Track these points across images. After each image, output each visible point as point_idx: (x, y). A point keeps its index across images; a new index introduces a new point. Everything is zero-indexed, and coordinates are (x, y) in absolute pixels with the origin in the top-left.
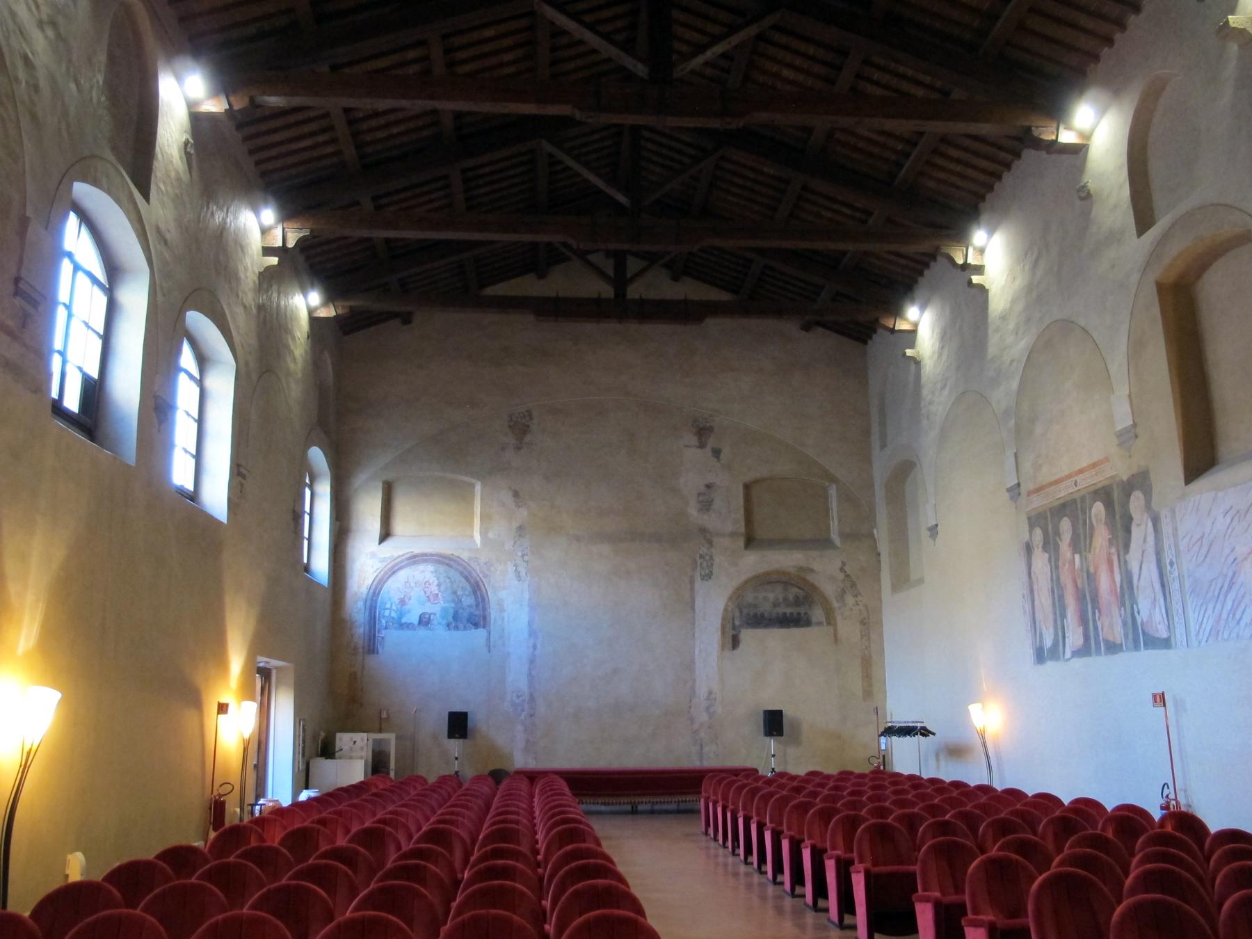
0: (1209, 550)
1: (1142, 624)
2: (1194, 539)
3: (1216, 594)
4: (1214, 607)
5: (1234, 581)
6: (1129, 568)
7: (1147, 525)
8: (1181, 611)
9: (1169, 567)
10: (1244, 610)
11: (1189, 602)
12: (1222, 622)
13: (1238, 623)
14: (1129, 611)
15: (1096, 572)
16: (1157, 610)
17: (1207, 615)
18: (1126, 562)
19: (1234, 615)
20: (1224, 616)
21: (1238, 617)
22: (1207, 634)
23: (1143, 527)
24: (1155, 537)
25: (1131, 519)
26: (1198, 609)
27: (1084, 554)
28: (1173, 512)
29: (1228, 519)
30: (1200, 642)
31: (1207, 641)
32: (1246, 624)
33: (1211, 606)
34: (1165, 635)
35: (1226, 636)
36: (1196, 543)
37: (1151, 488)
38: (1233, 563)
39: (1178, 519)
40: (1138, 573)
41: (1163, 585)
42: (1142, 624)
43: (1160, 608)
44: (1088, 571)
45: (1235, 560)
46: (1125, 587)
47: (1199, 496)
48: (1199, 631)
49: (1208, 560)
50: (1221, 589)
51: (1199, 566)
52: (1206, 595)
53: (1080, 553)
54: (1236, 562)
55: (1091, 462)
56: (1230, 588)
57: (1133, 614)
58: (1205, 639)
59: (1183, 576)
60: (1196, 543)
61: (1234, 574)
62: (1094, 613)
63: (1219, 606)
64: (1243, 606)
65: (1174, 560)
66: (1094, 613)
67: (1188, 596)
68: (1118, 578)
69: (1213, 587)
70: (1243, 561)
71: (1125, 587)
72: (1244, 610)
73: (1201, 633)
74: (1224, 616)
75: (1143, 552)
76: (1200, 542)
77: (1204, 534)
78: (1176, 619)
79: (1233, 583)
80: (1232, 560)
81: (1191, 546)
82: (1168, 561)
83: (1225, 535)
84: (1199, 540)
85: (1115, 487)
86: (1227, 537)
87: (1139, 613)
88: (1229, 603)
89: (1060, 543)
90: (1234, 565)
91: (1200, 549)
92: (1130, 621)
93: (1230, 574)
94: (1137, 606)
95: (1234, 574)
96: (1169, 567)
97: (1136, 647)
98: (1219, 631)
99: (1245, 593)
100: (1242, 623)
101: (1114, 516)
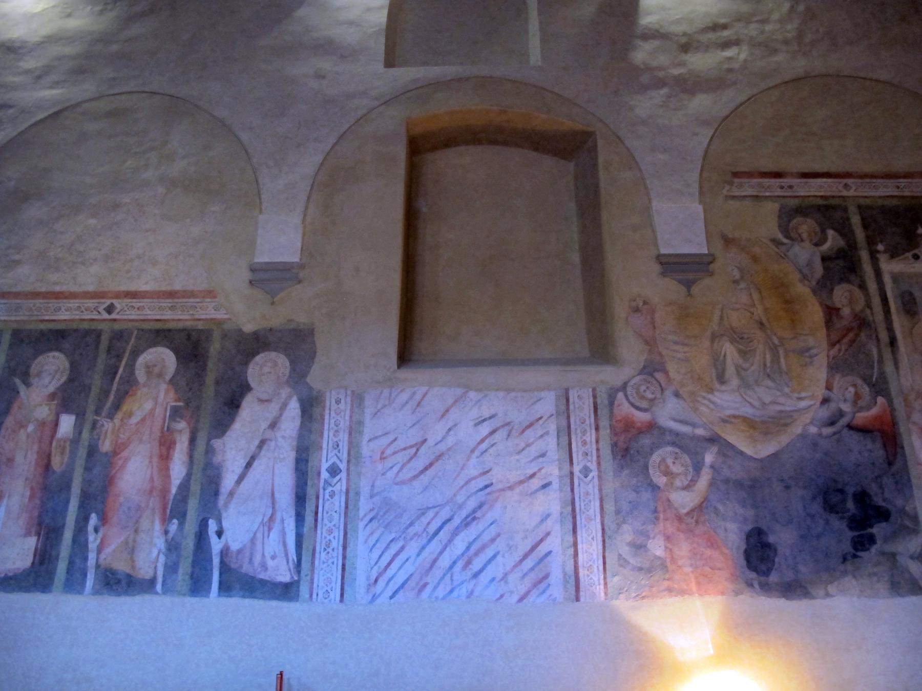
0: (431, 465)
1: (225, 552)
2: (401, 444)
3: (432, 528)
4: (423, 548)
5: (478, 514)
6: (217, 459)
7: (284, 406)
8: (337, 544)
9: (325, 475)
10: (494, 556)
11: (362, 535)
12: (437, 573)
13: (476, 575)
14: (191, 526)
15: (115, 453)
16: (274, 535)
17: (402, 557)
18: (210, 451)
19: (468, 563)
20: (445, 561)
21: (477, 565)
22: (393, 586)
23: (274, 408)
24: (303, 426)
25: (246, 388)
26: (381, 546)
27: (90, 417)
28: (358, 399)
29: (485, 429)
30: (374, 598)
31: (391, 598)
32: (493, 579)
33: (412, 549)
34: (284, 576)
35: (441, 592)
36: (405, 449)
37: (313, 355)
38: (481, 490)
39: (368, 412)
40: (239, 471)
41: (300, 499)
42: (225, 552)
43: (283, 533)
44: (92, 451)
45: (486, 487)
46: (195, 488)
47: (424, 389)
48: (376, 581)
49: (425, 478)
50: (444, 523)
51: (403, 483)
52: (407, 528)
53: (81, 416)
54: (489, 490)
55: (169, 288)
56: (468, 521)
57: (201, 537)
58: (389, 593)
59: (358, 494)
60: (405, 449)
61: (480, 506)
62: (83, 519)
63: (435, 546)
64: (489, 552)
65: (343, 466)
66: (83, 519)
67: (361, 525)
68: (178, 470)
69: (425, 520)
70: (503, 490)
71: (195, 488)
72: (494, 556)
73: (381, 583)
74: (445, 561)
75: (263, 443)
76: (414, 450)
77: (425, 440)
78: (321, 556)
79: (474, 519)
80: (481, 485)
81: (389, 452)
82: (325, 466)
83: (473, 451)
84: (411, 447)
85: (216, 335)
86: (477, 453)
87: (220, 534)
88: (460, 545)
89: (22, 389)
90: (481, 493)
91: (411, 459)
92: (189, 544)
93: (472, 504)
94: (219, 522)
95: (480, 506)
96: (325, 475)
97: (198, 586)
98: (426, 585)
99: (499, 535)
100: (484, 578)
101: (200, 374)
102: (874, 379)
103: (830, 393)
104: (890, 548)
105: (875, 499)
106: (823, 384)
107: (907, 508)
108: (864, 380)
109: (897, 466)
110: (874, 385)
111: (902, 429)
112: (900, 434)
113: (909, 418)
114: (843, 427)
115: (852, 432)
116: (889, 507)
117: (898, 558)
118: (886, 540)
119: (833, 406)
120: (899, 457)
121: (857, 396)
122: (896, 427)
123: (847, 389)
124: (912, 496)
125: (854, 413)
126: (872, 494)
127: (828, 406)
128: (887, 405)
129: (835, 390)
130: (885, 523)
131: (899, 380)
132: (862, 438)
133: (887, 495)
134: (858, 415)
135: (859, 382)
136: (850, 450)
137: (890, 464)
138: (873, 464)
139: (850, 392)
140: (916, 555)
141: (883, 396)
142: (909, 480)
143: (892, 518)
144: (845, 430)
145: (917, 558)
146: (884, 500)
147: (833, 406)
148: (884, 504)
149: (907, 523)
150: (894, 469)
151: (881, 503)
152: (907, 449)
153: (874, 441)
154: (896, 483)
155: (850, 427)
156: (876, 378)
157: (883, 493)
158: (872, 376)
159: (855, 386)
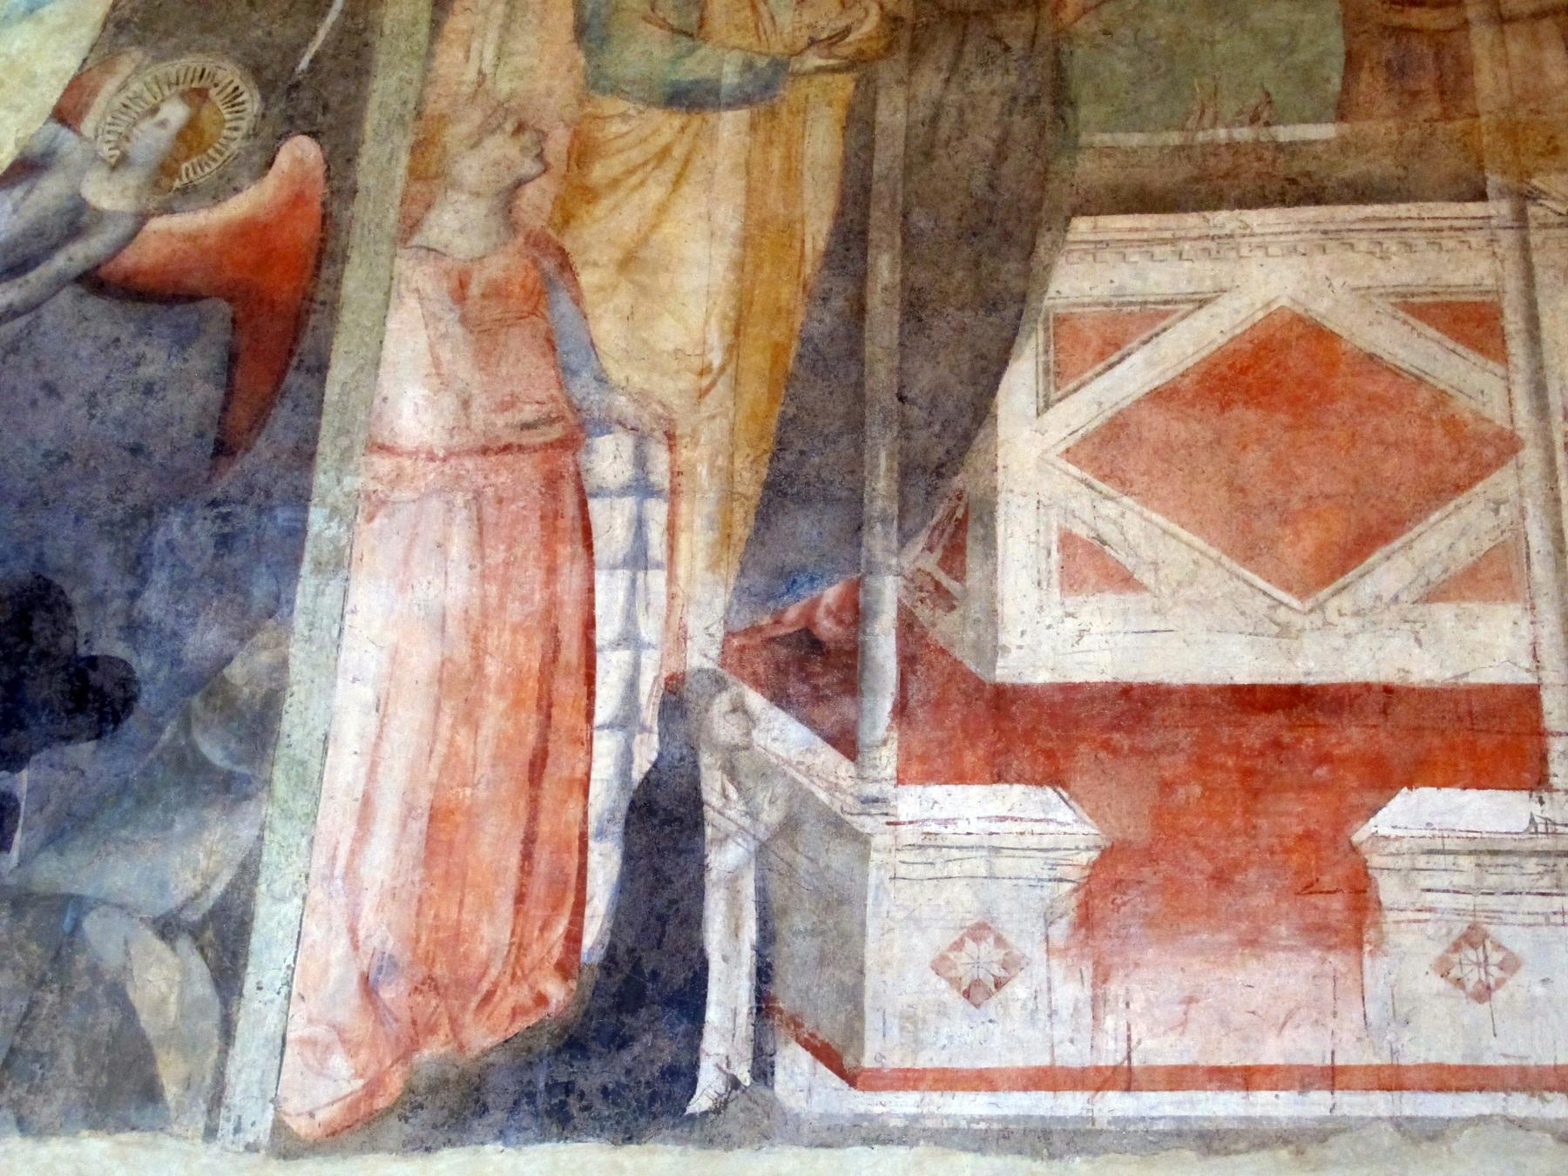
102: (304, 64)
103: (65, 133)
104: (51, 872)
105: (82, 622)
106: (51, 95)
107: (236, 672)
108: (256, 71)
109: (261, 456)
110: (296, 86)
111: (355, 281)
112: (333, 307)
113: (410, 226)
114: (60, 282)
115: (94, 305)
116: (144, 664)
117: (92, 925)
118: (57, 837)
119: (49, 191)
120: (282, 415)
121: (191, 138)
122: (326, 273)
123: (155, 110)
124: (279, 605)
125: (142, 218)
126: (77, 596)
127: (29, 192)
128: (319, 172)
129: (88, 126)
130: (89, 747)
131: (430, 55)
132: (126, 332)
133: (154, 603)
134: (157, 224)
135: (229, 73)
136: (51, 390)
137: (224, 449)
138: (136, 450)
139: (163, 124)
140: (193, 916)
141: (314, 135)
142: (297, 533)
143: (134, 726)
144: (65, 298)
145: (195, 932)
146: (133, 629)
147: (49, 191)
148: (120, 650)
149: (214, 750)
150: (228, 481)
151: (110, 644)
152: (339, 372)
153: (182, 341)
154: (224, 542)
155: (93, 281)
156: (315, 60)
157: (133, 595)
158: (297, 50)
159: (197, 96)
